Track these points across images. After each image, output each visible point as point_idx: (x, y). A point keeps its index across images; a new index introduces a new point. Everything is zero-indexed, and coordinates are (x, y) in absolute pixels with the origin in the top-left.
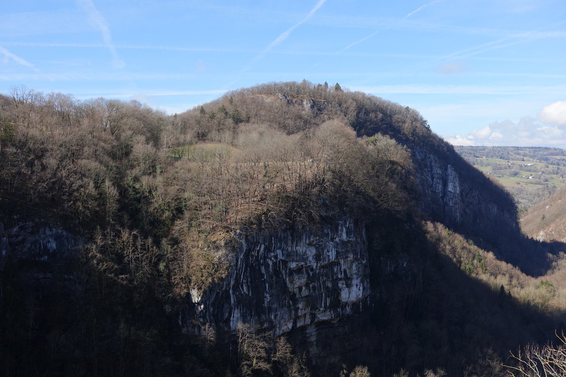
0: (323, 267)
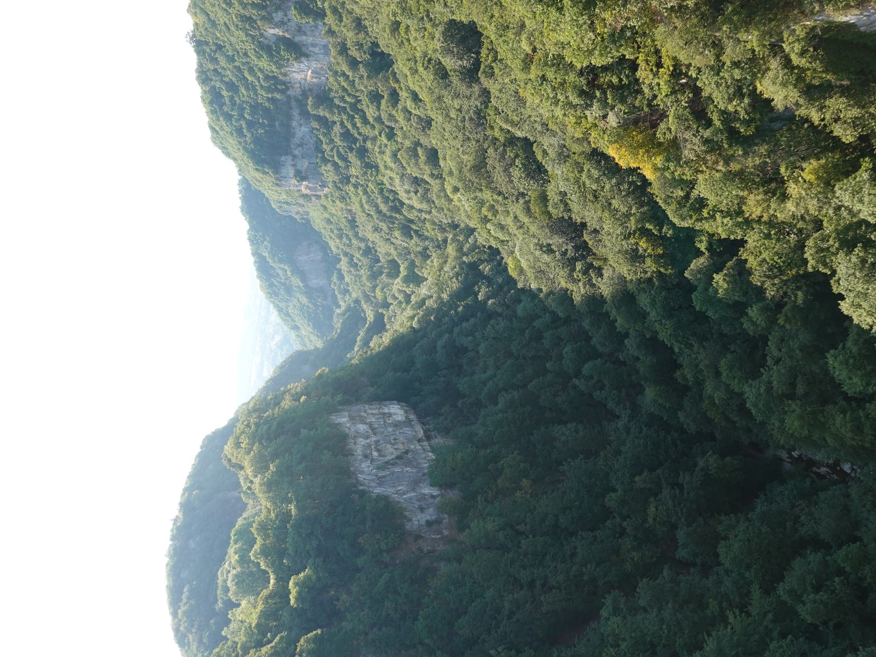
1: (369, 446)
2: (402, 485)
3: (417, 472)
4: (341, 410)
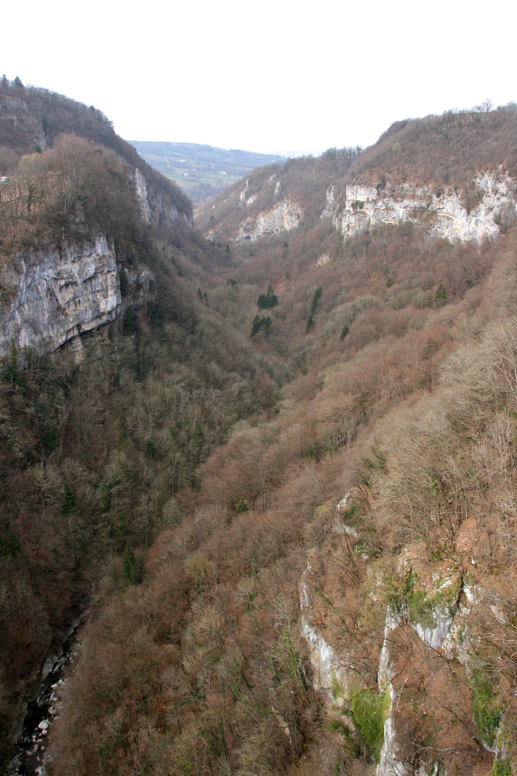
0: (85, 281)
1: (72, 277)
2: (29, 310)
3: (44, 325)
4: (110, 248)
